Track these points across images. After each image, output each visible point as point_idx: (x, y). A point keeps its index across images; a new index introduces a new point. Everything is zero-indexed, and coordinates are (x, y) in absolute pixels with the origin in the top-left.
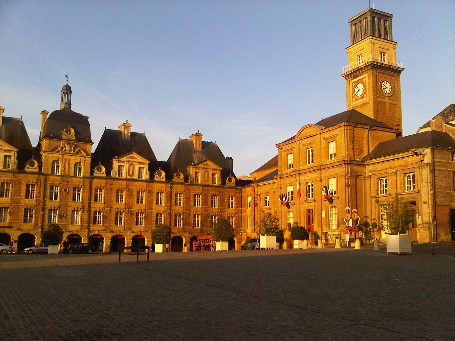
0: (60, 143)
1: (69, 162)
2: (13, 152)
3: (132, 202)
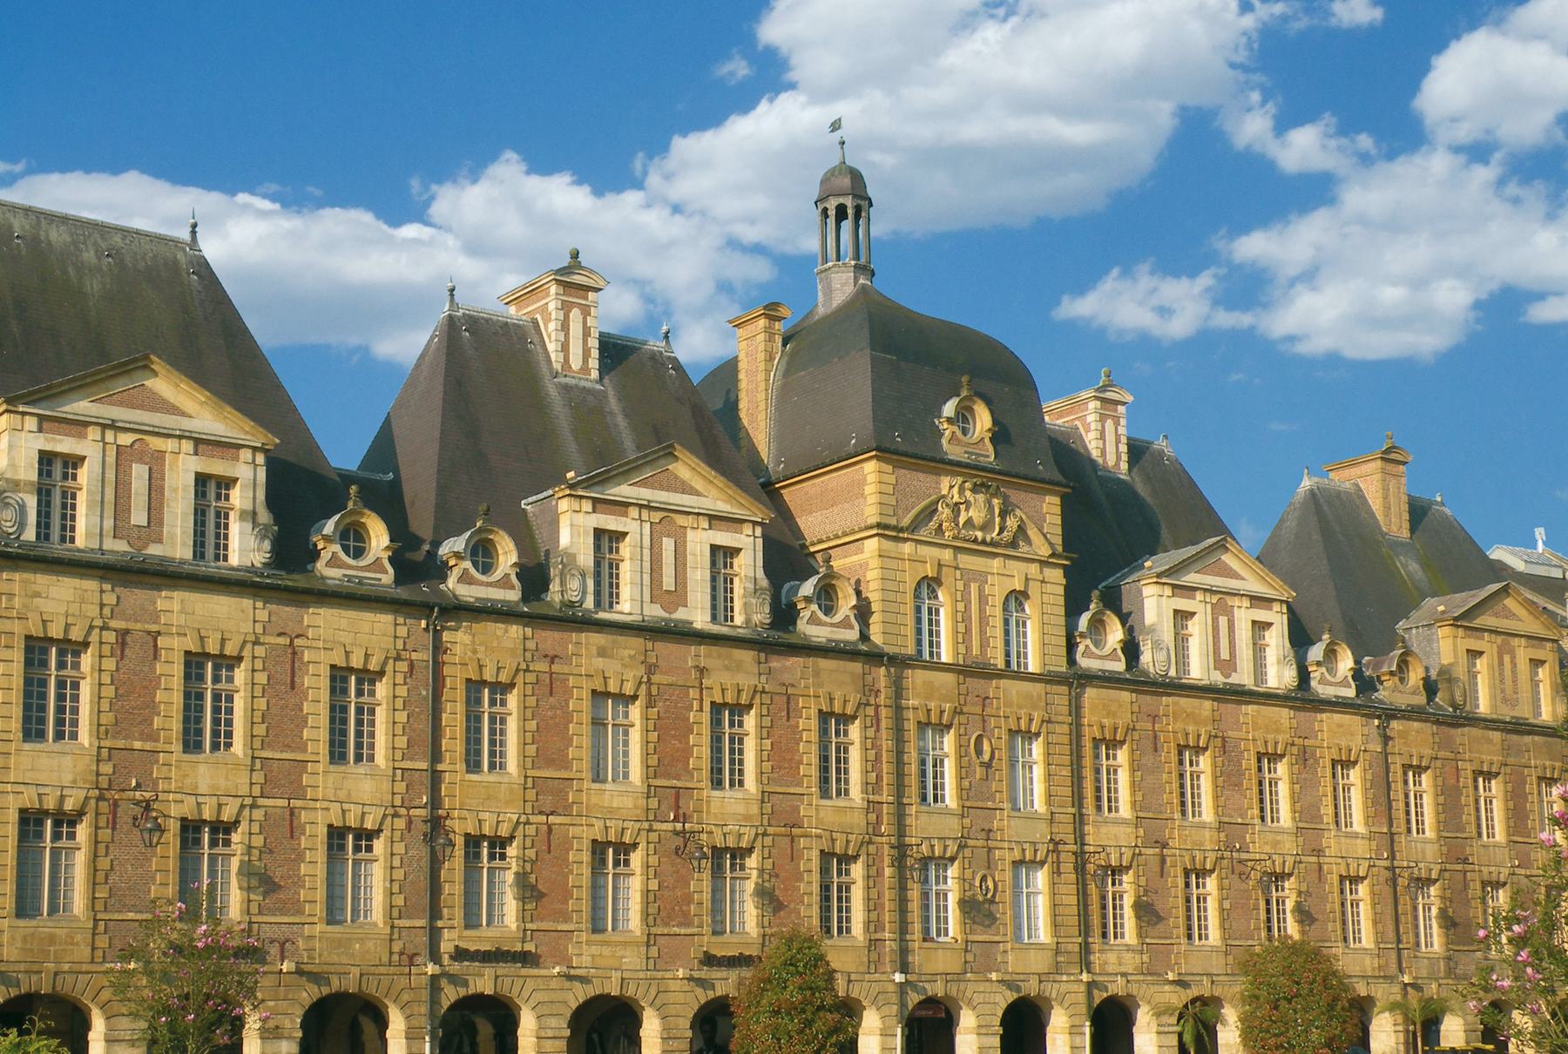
0: (938, 483)
1: (981, 590)
2: (748, 529)
3: (1241, 816)
